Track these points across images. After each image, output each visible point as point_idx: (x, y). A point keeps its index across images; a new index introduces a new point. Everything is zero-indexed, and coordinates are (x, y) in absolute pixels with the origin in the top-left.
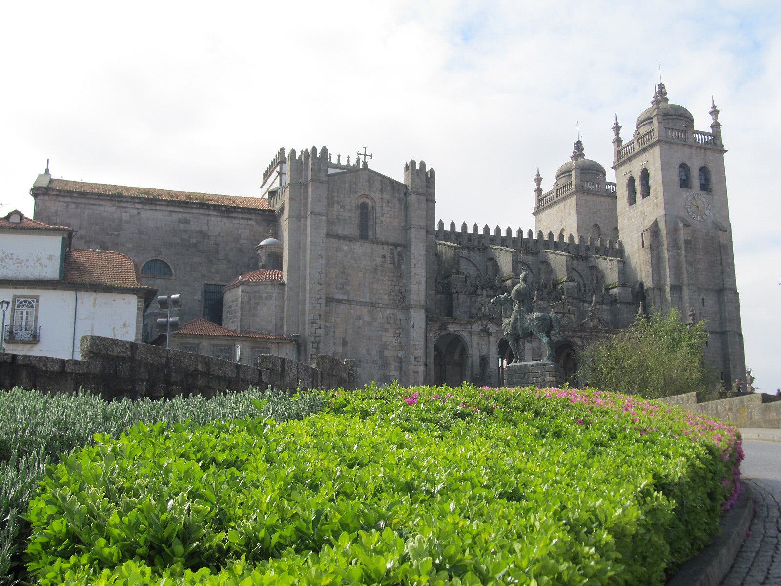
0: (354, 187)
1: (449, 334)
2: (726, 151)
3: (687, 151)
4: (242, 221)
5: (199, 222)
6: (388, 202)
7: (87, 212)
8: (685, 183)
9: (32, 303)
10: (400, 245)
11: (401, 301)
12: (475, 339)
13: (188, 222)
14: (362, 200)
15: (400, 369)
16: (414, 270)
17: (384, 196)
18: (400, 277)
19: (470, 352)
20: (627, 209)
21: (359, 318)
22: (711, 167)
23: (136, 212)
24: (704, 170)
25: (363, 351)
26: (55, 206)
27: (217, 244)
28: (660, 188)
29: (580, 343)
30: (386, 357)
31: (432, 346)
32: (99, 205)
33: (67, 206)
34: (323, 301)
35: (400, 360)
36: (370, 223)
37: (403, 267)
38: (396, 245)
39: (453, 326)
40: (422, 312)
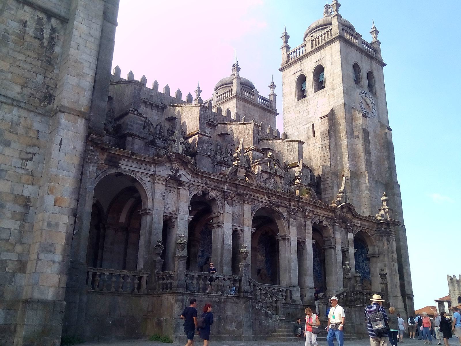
1: (120, 174)
2: (384, 65)
3: (359, 54)
8: (357, 81)
12: (160, 188)
18: (49, 62)
19: (150, 206)
20: (295, 104)
22: (375, 73)
24: (370, 75)
28: (339, 80)
29: (285, 215)
31: (90, 186)
37: (57, 49)
38: (50, 14)
39: (129, 163)
40: (80, 124)
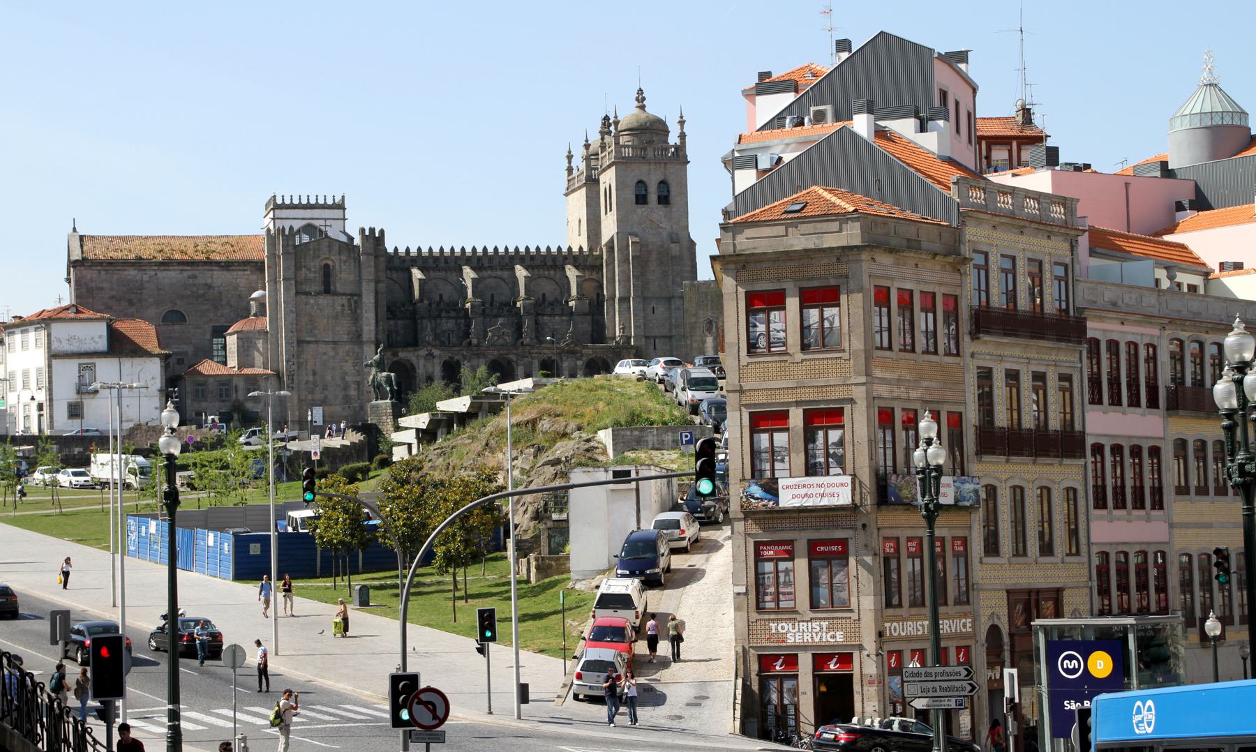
0: (317, 253)
4: (239, 273)
5: (204, 277)
6: (345, 262)
7: (115, 277)
9: (91, 368)
10: (356, 295)
11: (357, 339)
13: (195, 277)
14: (325, 262)
15: (358, 389)
16: (365, 315)
17: (342, 257)
18: (357, 319)
21: (325, 354)
23: (153, 273)
25: (329, 378)
26: (89, 274)
27: (220, 293)
29: (515, 359)
30: (347, 382)
32: (125, 270)
33: (99, 273)
34: (295, 344)
35: (358, 383)
36: (332, 279)
37: (358, 311)
